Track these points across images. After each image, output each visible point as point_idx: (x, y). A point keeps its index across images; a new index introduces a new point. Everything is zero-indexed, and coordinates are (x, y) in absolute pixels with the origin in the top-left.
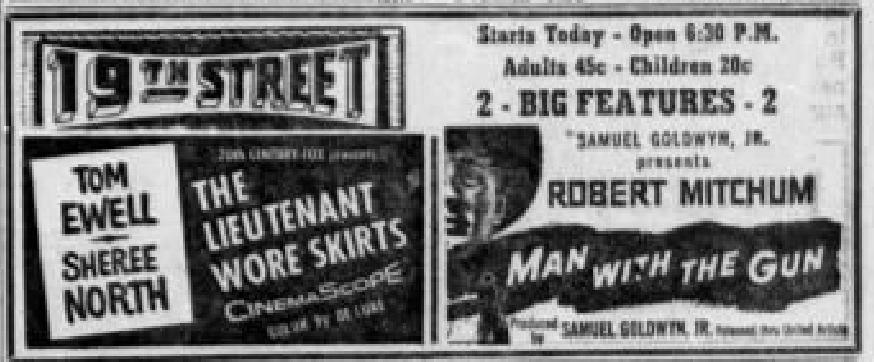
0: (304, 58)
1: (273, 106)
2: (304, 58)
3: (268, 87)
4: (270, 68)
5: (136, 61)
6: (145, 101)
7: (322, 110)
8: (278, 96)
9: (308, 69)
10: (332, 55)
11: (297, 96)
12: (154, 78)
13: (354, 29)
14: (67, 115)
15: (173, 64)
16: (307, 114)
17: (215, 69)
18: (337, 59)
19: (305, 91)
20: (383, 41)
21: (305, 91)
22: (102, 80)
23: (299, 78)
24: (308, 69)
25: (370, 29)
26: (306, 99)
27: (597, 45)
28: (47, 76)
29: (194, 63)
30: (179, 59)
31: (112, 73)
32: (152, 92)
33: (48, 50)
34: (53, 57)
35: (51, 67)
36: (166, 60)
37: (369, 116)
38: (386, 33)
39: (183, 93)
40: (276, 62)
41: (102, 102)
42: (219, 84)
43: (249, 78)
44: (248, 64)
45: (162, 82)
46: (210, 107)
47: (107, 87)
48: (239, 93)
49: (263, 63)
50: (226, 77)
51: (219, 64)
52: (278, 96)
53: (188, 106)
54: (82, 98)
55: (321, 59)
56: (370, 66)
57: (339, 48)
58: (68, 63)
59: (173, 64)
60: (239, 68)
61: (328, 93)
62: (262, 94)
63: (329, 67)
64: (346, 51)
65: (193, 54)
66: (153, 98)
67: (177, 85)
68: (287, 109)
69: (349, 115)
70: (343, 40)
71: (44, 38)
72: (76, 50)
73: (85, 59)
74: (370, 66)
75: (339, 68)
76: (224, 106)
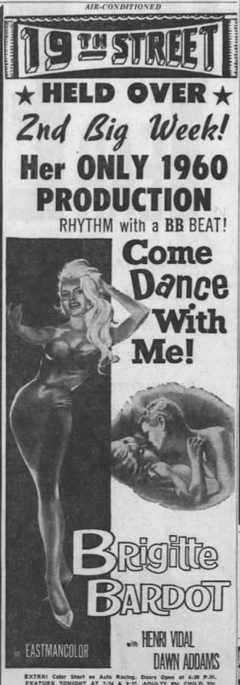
0: (179, 32)
1: (159, 64)
3: (156, 50)
4: (157, 39)
5: (75, 34)
6: (80, 60)
8: (162, 57)
10: (195, 30)
11: (173, 58)
12: (86, 45)
13: (209, 15)
14: (33, 69)
15: (97, 36)
16: (179, 68)
18: (198, 33)
19: (178, 53)
20: (226, 23)
21: (178, 53)
22: (54, 47)
24: (178, 39)
25: (219, 15)
28: (21, 43)
29: (110, 35)
30: (101, 33)
31: (60, 41)
32: (84, 54)
33: (21, 27)
34: (24, 33)
35: (22, 38)
36: (93, 33)
37: (218, 69)
38: (227, 17)
39: (104, 54)
40: (161, 35)
41: (54, 60)
42: (125, 47)
44: (143, 35)
45: (90, 48)
48: (138, 56)
50: (129, 43)
52: (162, 57)
53: (106, 63)
54: (42, 58)
55: (188, 33)
56: (218, 37)
57: (199, 27)
58: (33, 36)
59: (97, 36)
60: (137, 38)
61: (193, 55)
62: (152, 56)
63: (193, 38)
64: (203, 28)
66: (84, 58)
67: (99, 49)
68: (167, 65)
69: (206, 69)
73: (43, 33)
74: (218, 37)
75: (198, 39)
76: (128, 64)
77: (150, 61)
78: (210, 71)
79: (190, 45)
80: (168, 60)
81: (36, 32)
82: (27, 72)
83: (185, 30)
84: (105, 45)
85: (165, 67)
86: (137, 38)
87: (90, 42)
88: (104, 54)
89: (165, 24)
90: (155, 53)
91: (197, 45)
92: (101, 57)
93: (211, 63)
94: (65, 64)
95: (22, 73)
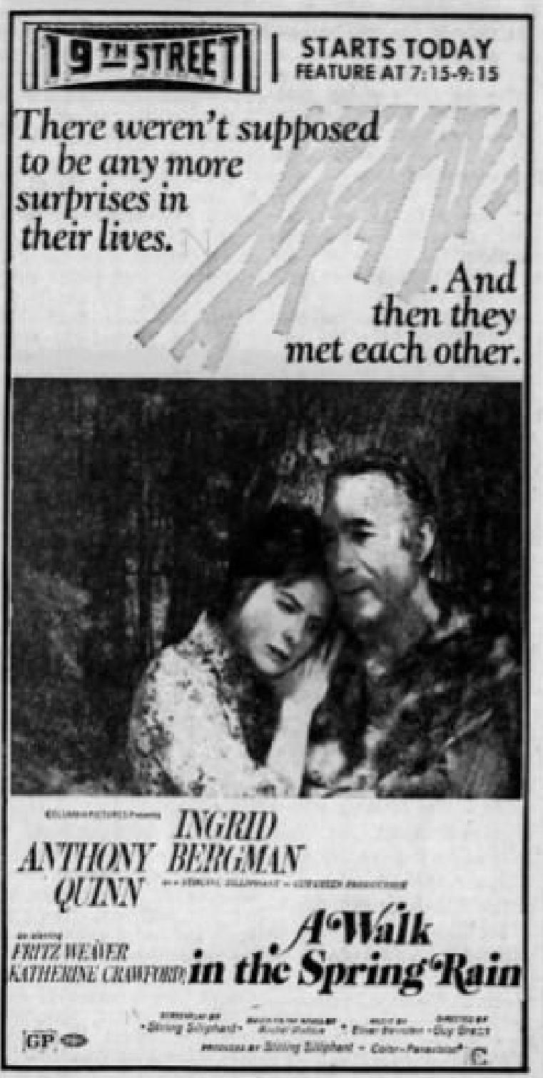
4: (176, 50)
5: (96, 44)
7: (207, 80)
8: (181, 69)
9: (199, 50)
10: (213, 41)
12: (106, 54)
14: (52, 80)
15: (118, 46)
19: (199, 64)
20: (247, 34)
22: (74, 56)
23: (193, 57)
24: (199, 50)
26: (196, 71)
29: (131, 45)
30: (121, 42)
31: (80, 51)
32: (106, 65)
33: (42, 34)
36: (114, 42)
37: (237, 83)
39: (123, 65)
40: (179, 45)
41: (76, 70)
42: (144, 56)
43: (165, 55)
45: (112, 57)
48: (158, 66)
49: (173, 45)
50: (151, 54)
51: (146, 46)
52: (181, 69)
55: (207, 43)
57: (218, 37)
59: (118, 46)
60: (158, 48)
61: (212, 66)
62: (172, 67)
63: (213, 49)
65: (131, 38)
67: (121, 60)
71: (39, 27)
72: (59, 35)
73: (65, 42)
75: (219, 50)
76: (147, 74)
79: (209, 57)
82: (47, 82)
86: (158, 48)
87: (112, 53)
89: (185, 32)
95: (41, 84)
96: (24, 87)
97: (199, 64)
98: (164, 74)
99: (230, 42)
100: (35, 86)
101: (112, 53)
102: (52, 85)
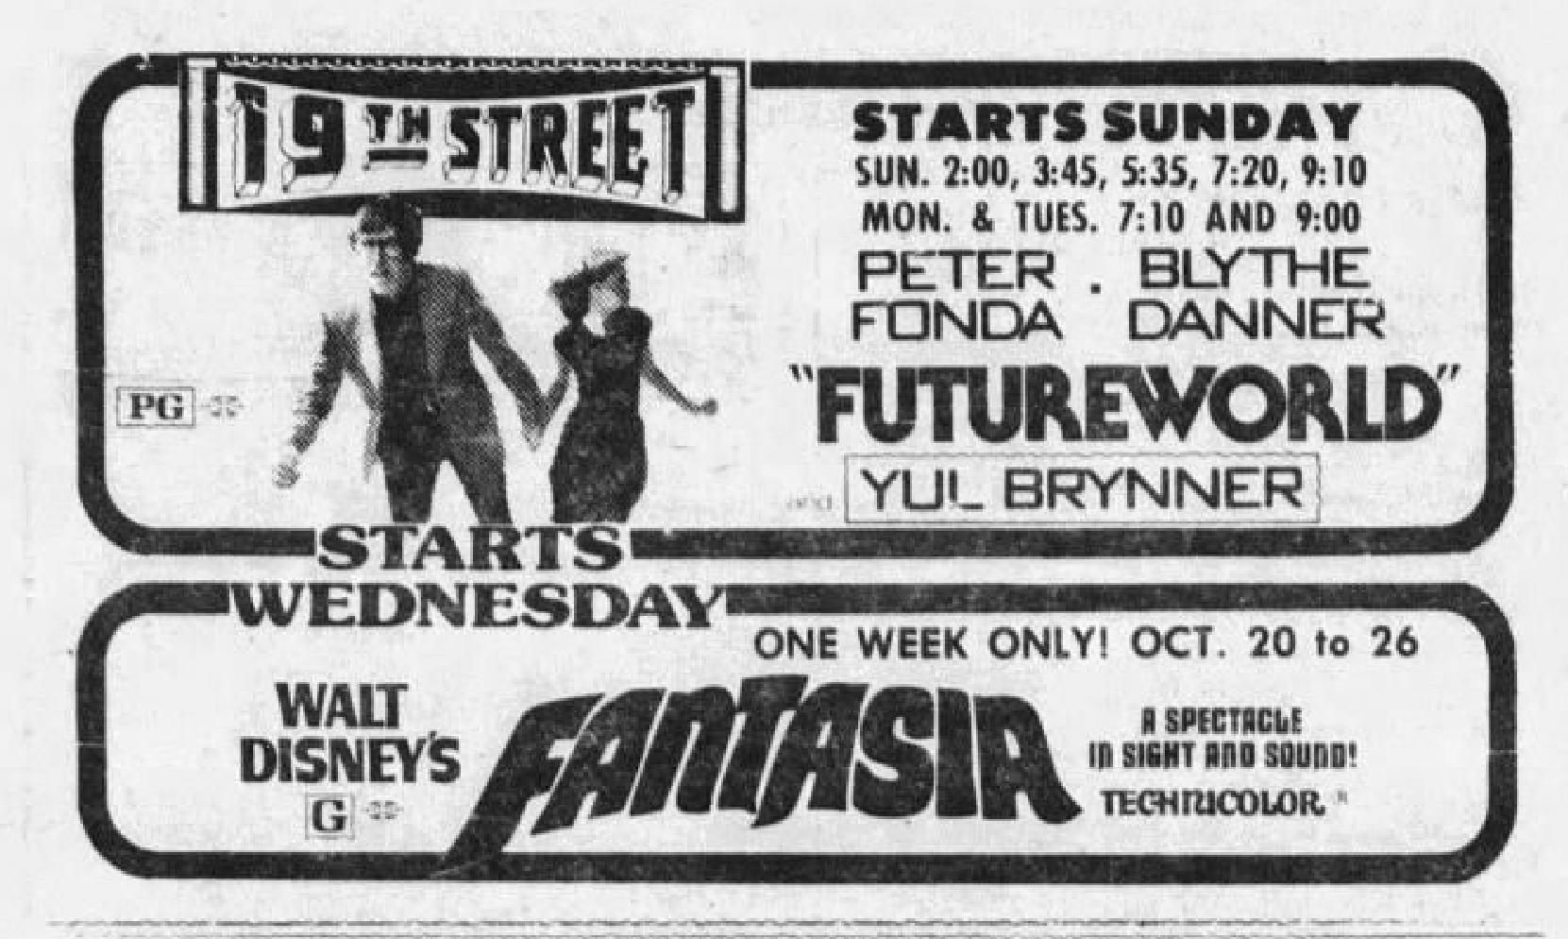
0: (601, 106)
1: (553, 182)
2: (601, 106)
4: (549, 123)
5: (355, 108)
6: (367, 168)
7: (625, 192)
8: (560, 167)
9: (603, 124)
10: (639, 102)
11: (587, 168)
12: (381, 133)
13: (672, 64)
14: (253, 187)
15: (407, 111)
16: (603, 195)
17: (471, 121)
19: (602, 156)
22: (303, 134)
24: (603, 124)
25: (698, 63)
26: (598, 172)
27: (1216, 208)
29: (440, 112)
30: (416, 105)
31: (318, 122)
32: (376, 156)
33: (226, 83)
36: (398, 105)
37: (693, 199)
38: (715, 71)
39: (422, 156)
40: (559, 113)
41: (304, 167)
42: (472, 141)
43: (520, 134)
44: (517, 113)
45: (391, 142)
46: (461, 180)
47: (314, 144)
48: (503, 161)
51: (475, 114)
52: (560, 167)
55: (623, 108)
56: (695, 118)
57: (650, 93)
59: (407, 111)
60: (503, 119)
62: (536, 163)
63: (636, 120)
64: (662, 98)
67: (413, 144)
68: (572, 185)
69: (664, 198)
70: (654, 79)
73: (280, 101)
74: (695, 118)
75: (649, 122)
76: (479, 179)
77: (533, 175)
78: (675, 202)
79: (628, 138)
80: (575, 172)
81: (261, 97)
83: (617, 101)
84: (425, 134)
85: (568, 191)
86: (503, 119)
87: (394, 126)
88: (422, 156)
90: (543, 157)
91: (646, 138)
92: (417, 163)
93: (677, 183)
94: (329, 177)
96: (185, 205)
97: (602, 156)
98: (518, 179)
99: (675, 104)
100: (211, 204)
101: (394, 126)
102: (247, 202)
